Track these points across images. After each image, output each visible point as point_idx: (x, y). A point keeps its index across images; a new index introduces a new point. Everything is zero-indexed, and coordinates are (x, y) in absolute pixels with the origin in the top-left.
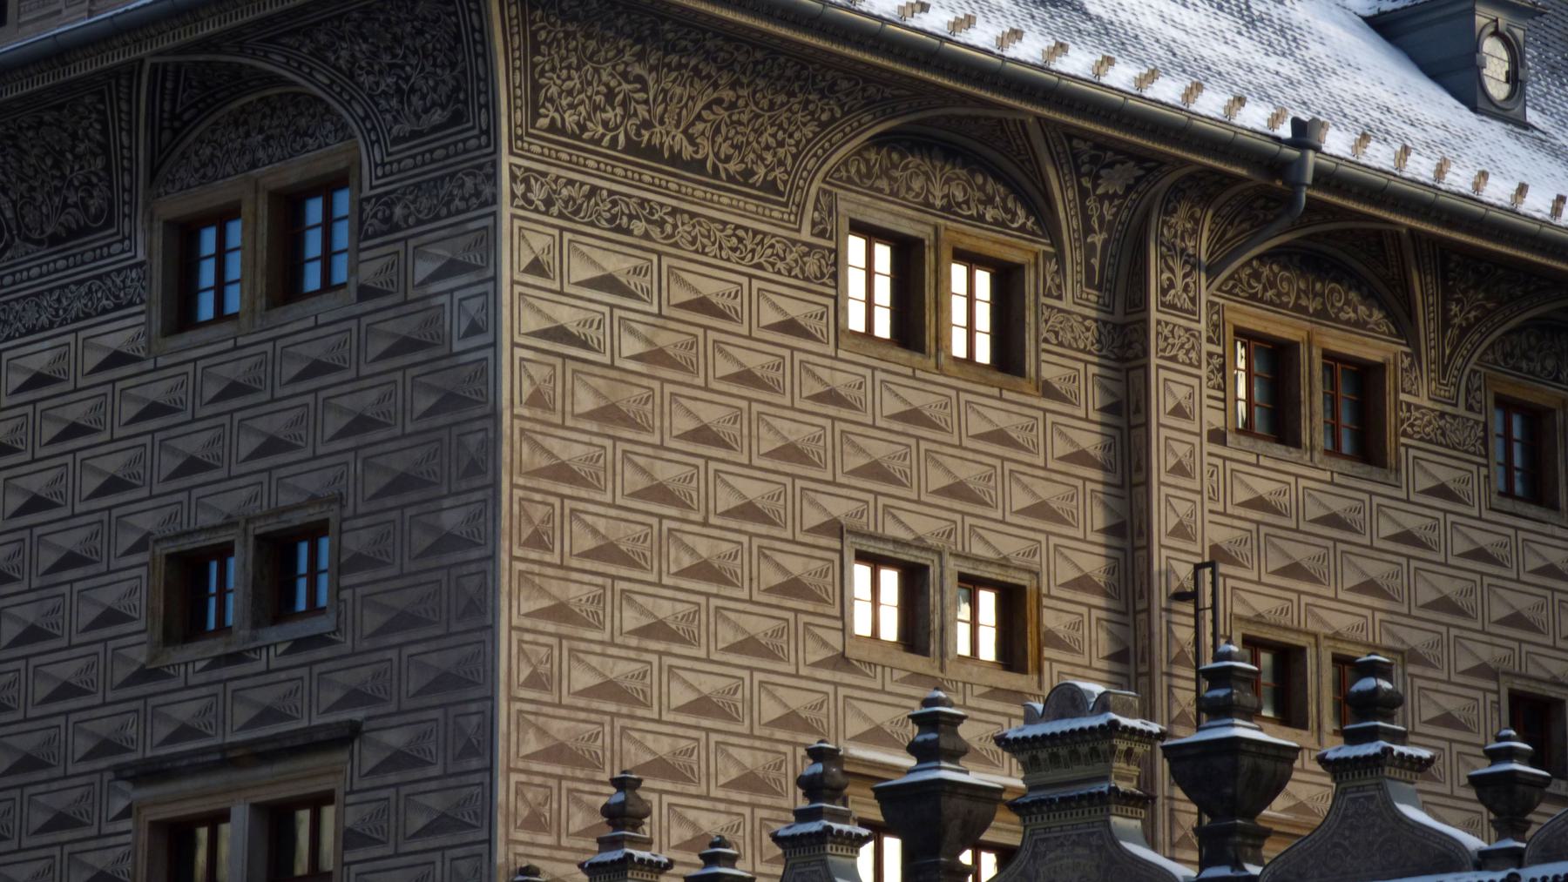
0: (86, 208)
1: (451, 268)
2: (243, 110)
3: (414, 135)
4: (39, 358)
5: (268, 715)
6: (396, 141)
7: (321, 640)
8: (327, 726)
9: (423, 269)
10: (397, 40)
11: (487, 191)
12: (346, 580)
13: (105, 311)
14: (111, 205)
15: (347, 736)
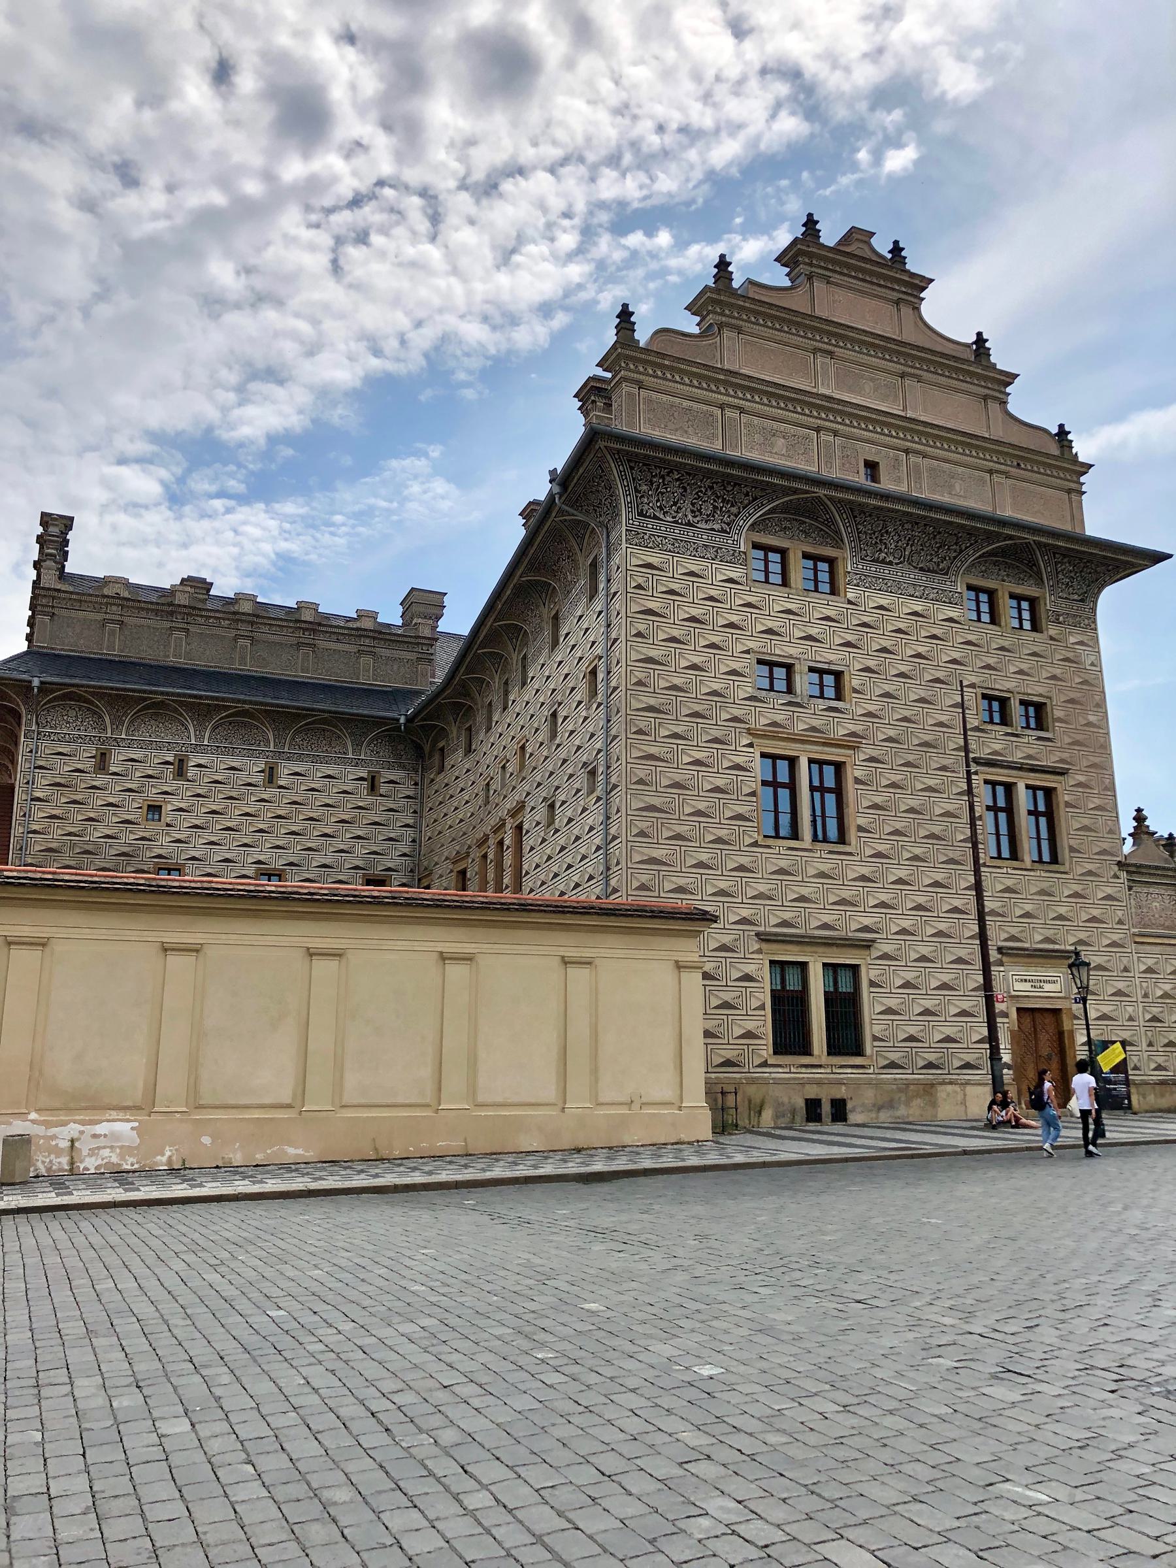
0: (938, 565)
1: (1081, 643)
2: (997, 561)
3: (1066, 598)
4: (918, 608)
5: (1029, 757)
6: (1059, 597)
7: (1048, 739)
8: (1049, 767)
9: (1072, 640)
10: (1081, 572)
11: (1093, 626)
12: (1057, 724)
13: (944, 602)
14: (949, 568)
15: (1062, 773)
